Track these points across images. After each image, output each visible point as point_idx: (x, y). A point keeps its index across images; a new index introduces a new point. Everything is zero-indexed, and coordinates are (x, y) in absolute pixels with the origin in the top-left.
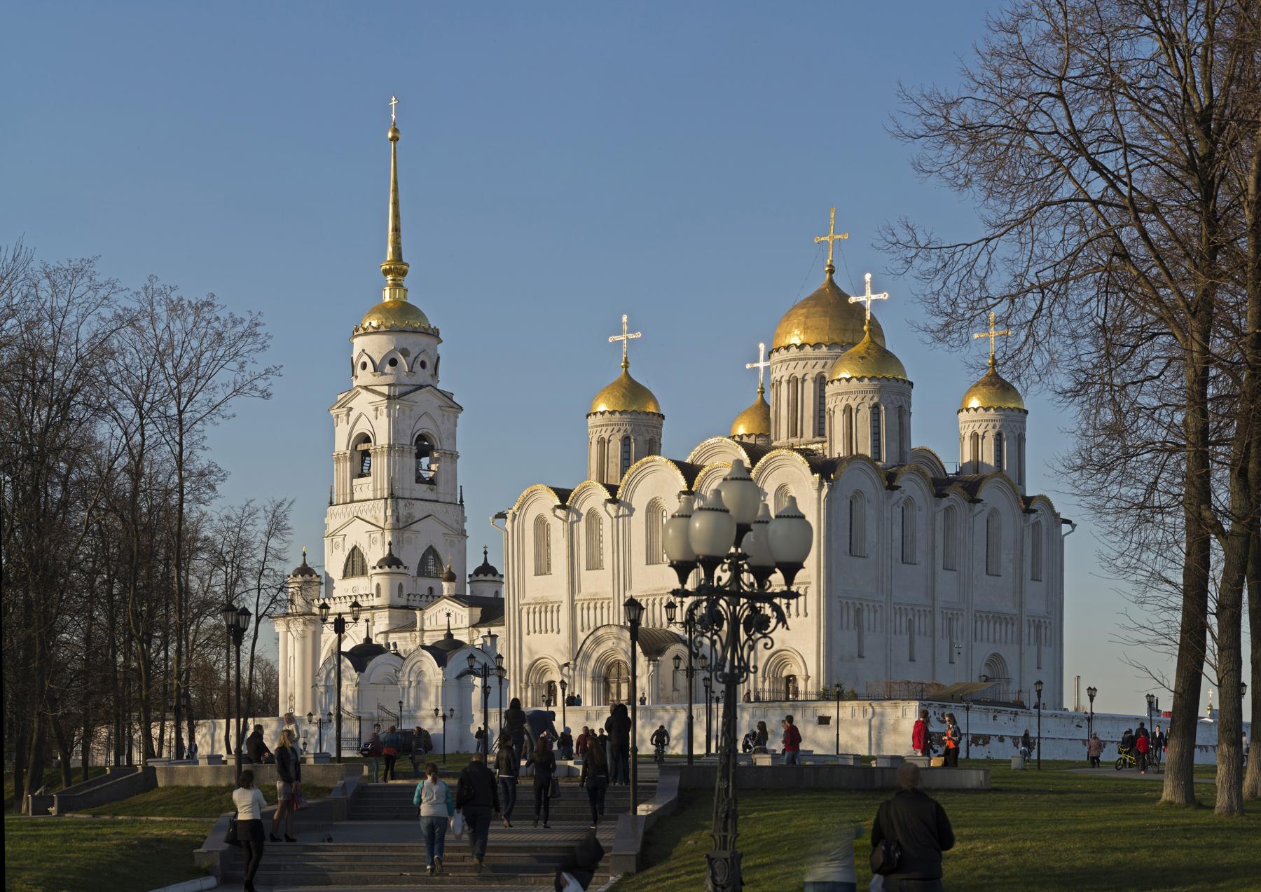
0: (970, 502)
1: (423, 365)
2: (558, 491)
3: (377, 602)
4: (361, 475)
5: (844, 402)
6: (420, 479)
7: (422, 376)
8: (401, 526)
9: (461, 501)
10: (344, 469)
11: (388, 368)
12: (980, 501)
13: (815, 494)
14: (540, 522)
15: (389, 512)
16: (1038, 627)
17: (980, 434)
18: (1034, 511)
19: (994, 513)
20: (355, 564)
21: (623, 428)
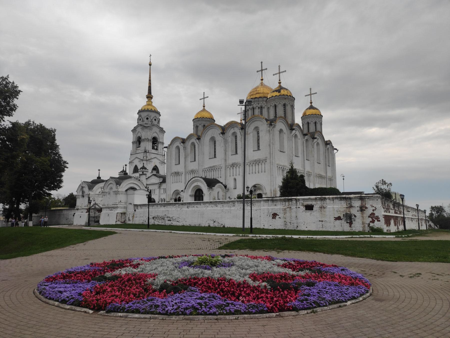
1: (155, 120)
5: (274, 104)
6: (153, 148)
7: (155, 123)
11: (145, 120)
12: (316, 138)
19: (318, 144)
20: (136, 170)
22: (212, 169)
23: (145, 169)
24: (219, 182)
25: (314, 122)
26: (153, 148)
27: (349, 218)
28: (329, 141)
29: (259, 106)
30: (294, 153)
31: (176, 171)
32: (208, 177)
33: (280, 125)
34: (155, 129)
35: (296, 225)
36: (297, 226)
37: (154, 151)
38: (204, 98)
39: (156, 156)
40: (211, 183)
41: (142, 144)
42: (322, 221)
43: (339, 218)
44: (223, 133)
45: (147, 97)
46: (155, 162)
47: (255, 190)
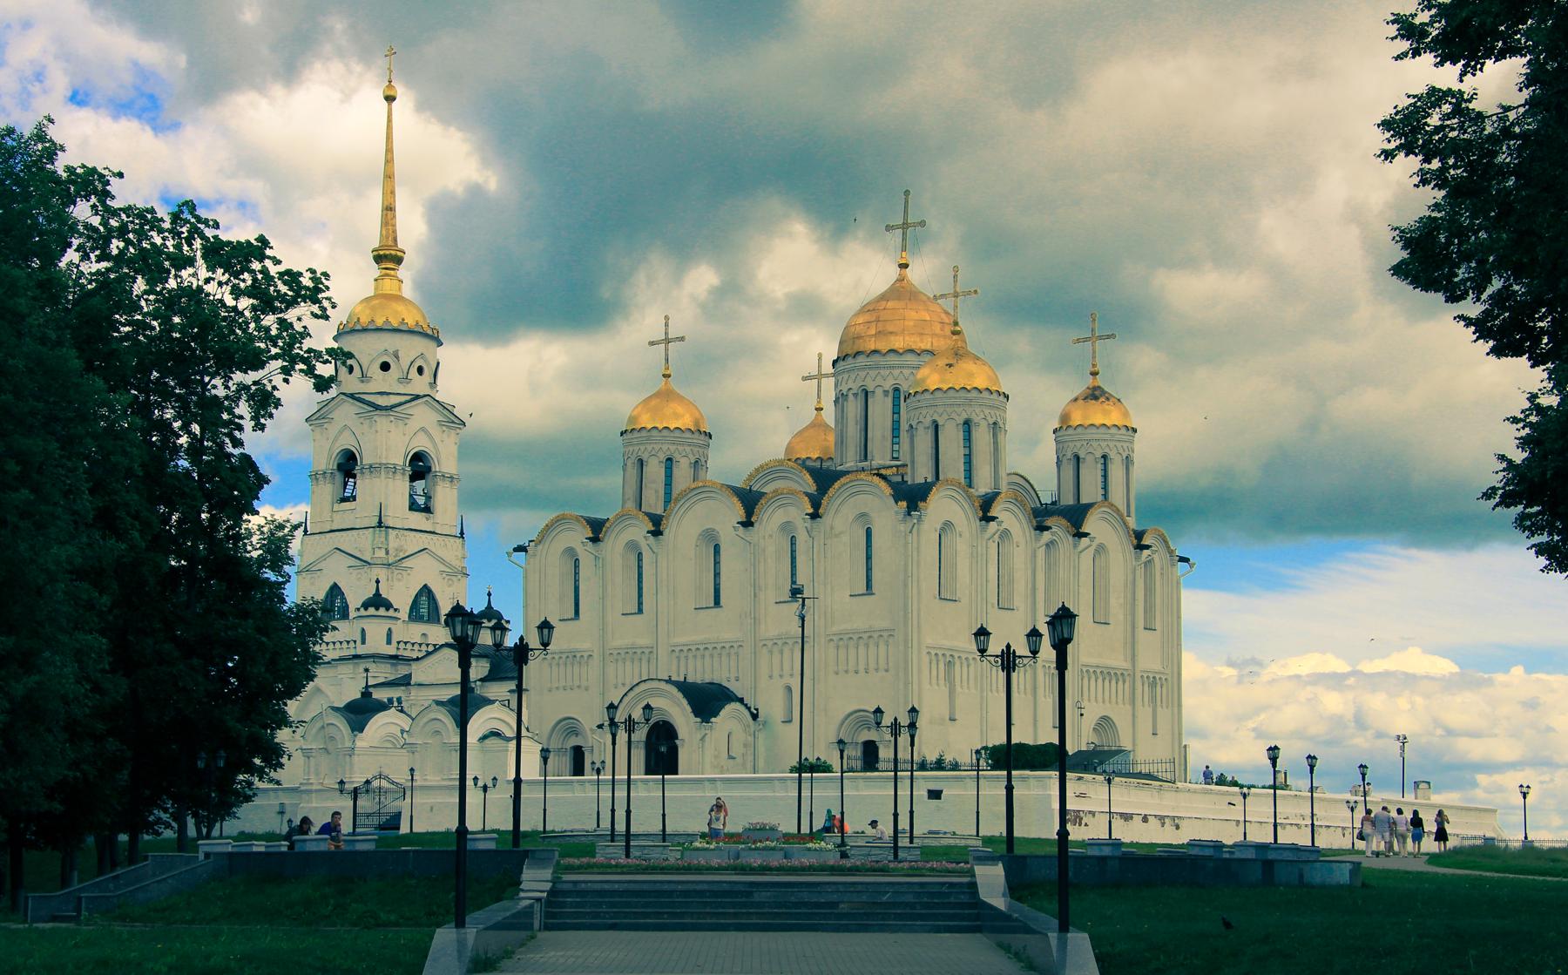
1: (420, 370)
3: (361, 650)
4: (344, 500)
6: (413, 507)
7: (419, 385)
9: (462, 533)
11: (375, 371)
16: (1153, 684)
18: (1147, 547)
19: (1101, 549)
21: (665, 447)
23: (388, 605)
25: (1099, 455)
26: (413, 507)
29: (888, 385)
32: (690, 680)
33: (943, 506)
34: (422, 415)
37: (418, 520)
38: (667, 341)
40: (707, 700)
41: (364, 486)
44: (747, 524)
45: (379, 259)
46: (423, 572)
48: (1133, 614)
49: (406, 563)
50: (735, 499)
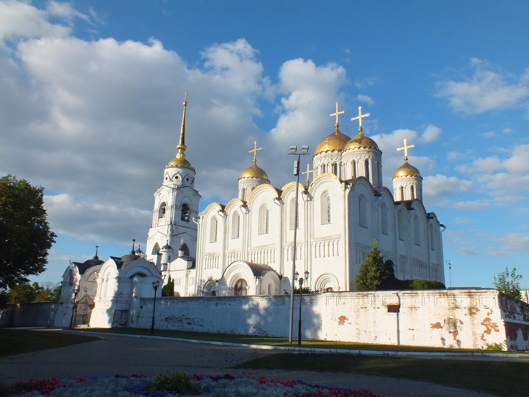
0: (408, 209)
1: (188, 179)
2: (221, 205)
5: (352, 159)
8: (173, 235)
10: (156, 215)
11: (174, 179)
12: (413, 209)
13: (343, 193)
14: (214, 218)
15: (169, 230)
17: (404, 186)
19: (416, 217)
22: (263, 249)
24: (271, 269)
26: (183, 219)
27: (454, 325)
28: (433, 213)
29: (332, 162)
30: (380, 229)
31: (210, 251)
35: (373, 335)
36: (376, 337)
37: (183, 223)
39: (185, 230)
42: (413, 330)
43: (438, 326)
47: (307, 278)
48: (428, 243)
49: (179, 236)
50: (275, 190)
